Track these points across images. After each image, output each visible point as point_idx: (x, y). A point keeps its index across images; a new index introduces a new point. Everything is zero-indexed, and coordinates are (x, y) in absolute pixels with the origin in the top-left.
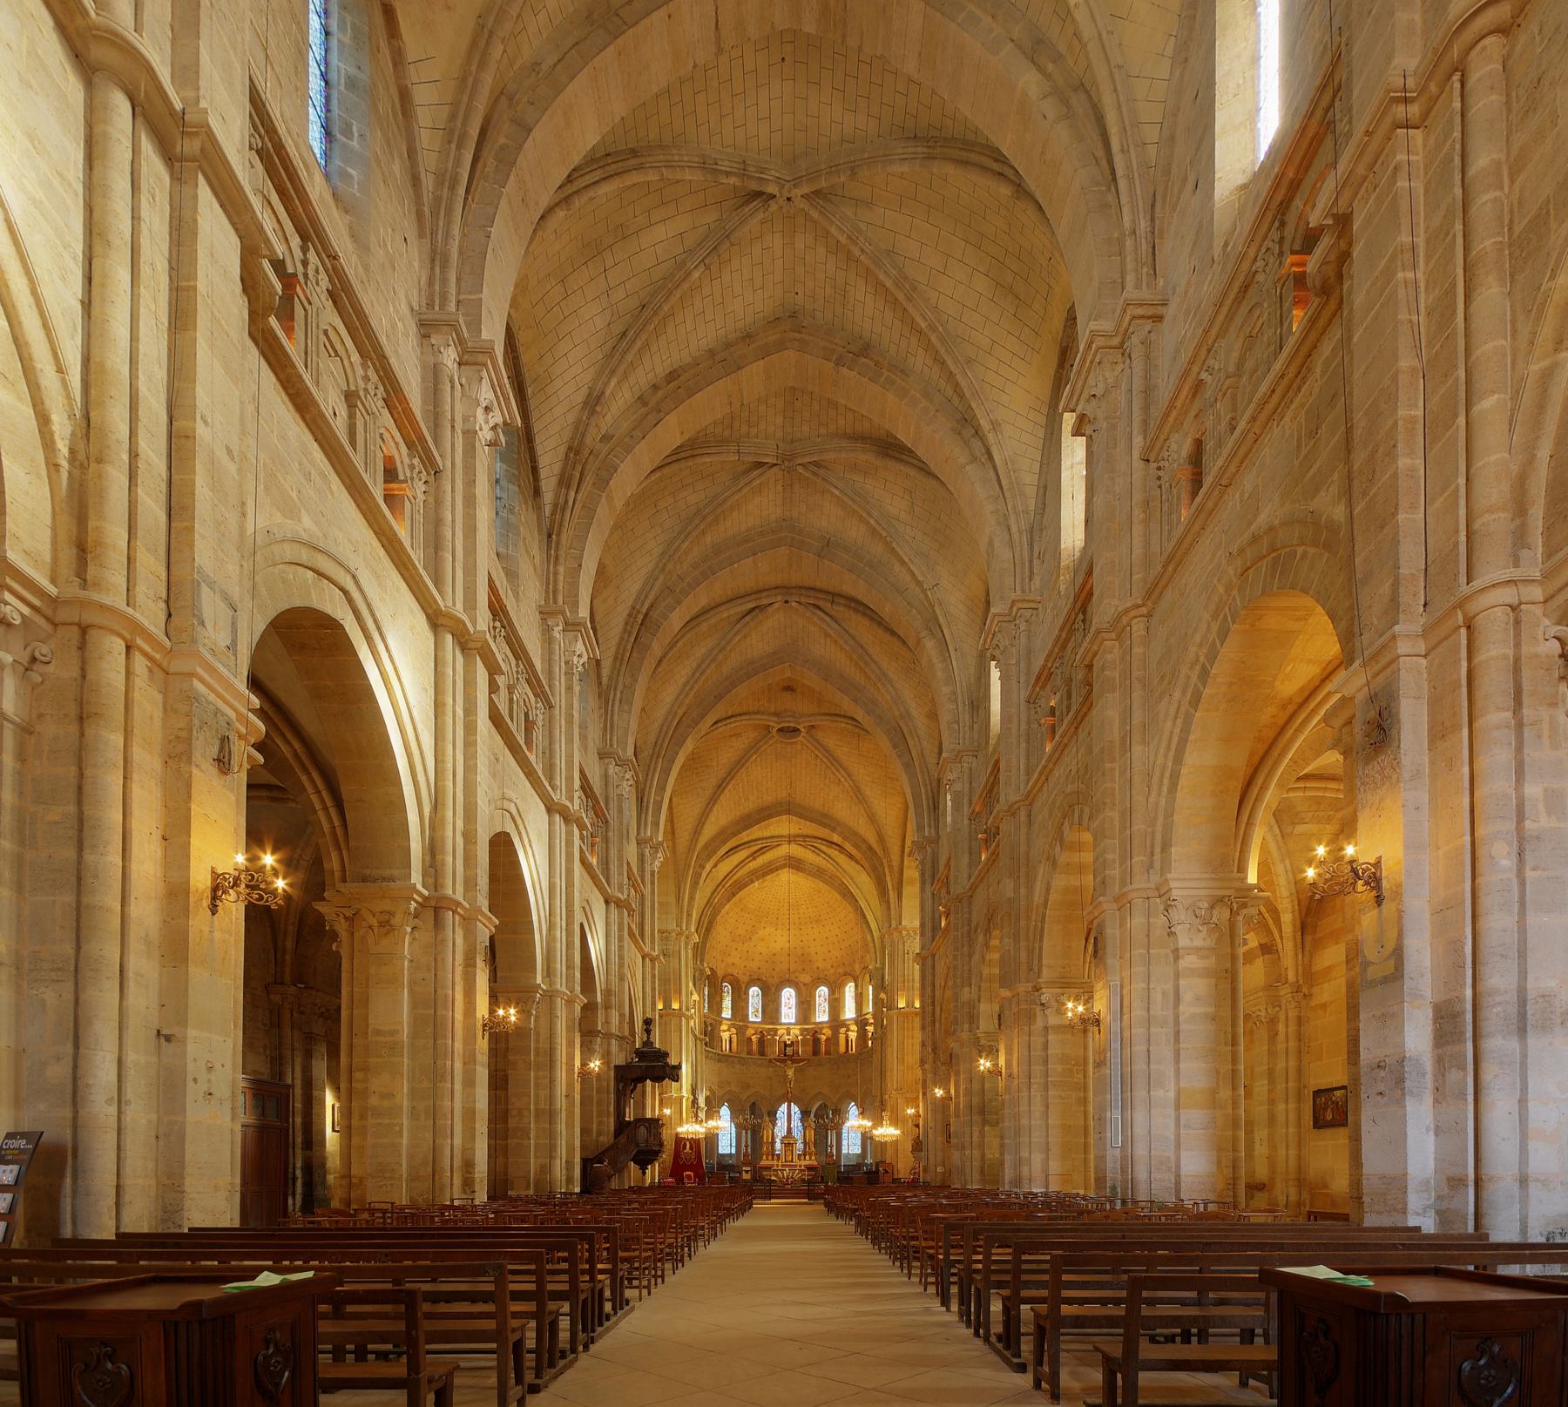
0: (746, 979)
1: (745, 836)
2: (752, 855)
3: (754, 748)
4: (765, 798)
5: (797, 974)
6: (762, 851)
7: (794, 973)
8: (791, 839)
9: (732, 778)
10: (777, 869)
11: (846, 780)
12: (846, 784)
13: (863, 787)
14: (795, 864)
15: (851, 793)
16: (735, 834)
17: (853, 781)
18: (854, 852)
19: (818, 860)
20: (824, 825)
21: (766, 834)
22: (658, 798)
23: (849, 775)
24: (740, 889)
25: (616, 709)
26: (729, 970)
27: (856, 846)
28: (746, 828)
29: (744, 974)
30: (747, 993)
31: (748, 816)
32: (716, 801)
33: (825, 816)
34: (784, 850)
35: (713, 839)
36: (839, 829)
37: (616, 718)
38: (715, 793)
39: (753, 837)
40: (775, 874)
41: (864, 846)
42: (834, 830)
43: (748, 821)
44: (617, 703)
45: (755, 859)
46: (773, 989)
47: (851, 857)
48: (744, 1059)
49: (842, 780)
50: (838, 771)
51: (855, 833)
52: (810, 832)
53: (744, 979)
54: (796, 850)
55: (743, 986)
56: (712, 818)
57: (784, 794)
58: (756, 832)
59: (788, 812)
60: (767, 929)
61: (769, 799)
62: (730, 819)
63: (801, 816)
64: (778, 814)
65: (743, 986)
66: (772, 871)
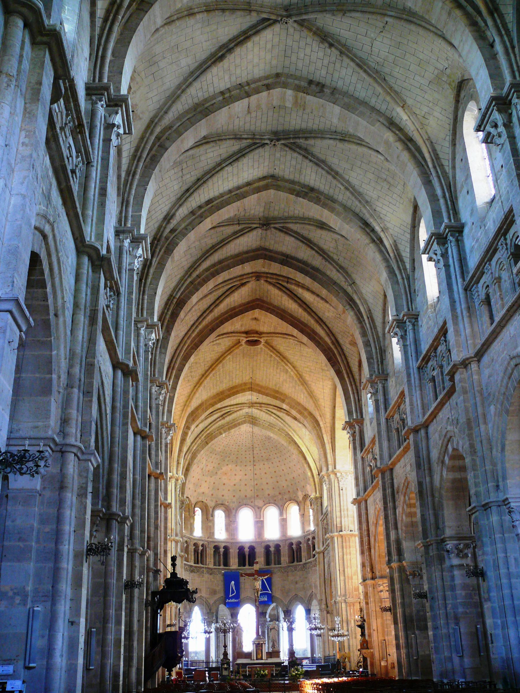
0: (212, 504)
1: (219, 406)
2: (222, 416)
3: (229, 350)
4: (234, 380)
5: (253, 500)
6: (228, 413)
7: (250, 498)
8: (252, 405)
9: (213, 370)
10: (239, 424)
11: (292, 370)
12: (292, 373)
13: (304, 375)
14: (253, 421)
15: (296, 379)
16: (212, 405)
17: (297, 371)
18: (298, 416)
19: (272, 419)
20: (276, 398)
21: (232, 402)
22: (172, 395)
23: (293, 367)
24: (212, 440)
25: (158, 352)
26: (200, 499)
27: (300, 413)
28: (221, 400)
29: (212, 501)
30: (213, 516)
31: (222, 393)
32: (200, 385)
33: (277, 392)
34: (246, 410)
35: (197, 409)
36: (287, 401)
37: (157, 358)
38: (200, 379)
39: (224, 406)
40: (238, 428)
41: (306, 413)
42: (283, 401)
43: (222, 396)
44: (159, 349)
45: (224, 418)
46: (234, 511)
47: (295, 418)
48: (211, 569)
49: (290, 370)
50: (287, 365)
51: (299, 404)
52: (264, 401)
53: (211, 504)
54: (255, 412)
55: (211, 510)
56: (197, 395)
57: (248, 378)
58: (227, 402)
59: (251, 389)
60: (230, 466)
61: (237, 381)
62: (209, 394)
63: (259, 392)
64: (243, 391)
65: (211, 510)
66: (235, 426)
